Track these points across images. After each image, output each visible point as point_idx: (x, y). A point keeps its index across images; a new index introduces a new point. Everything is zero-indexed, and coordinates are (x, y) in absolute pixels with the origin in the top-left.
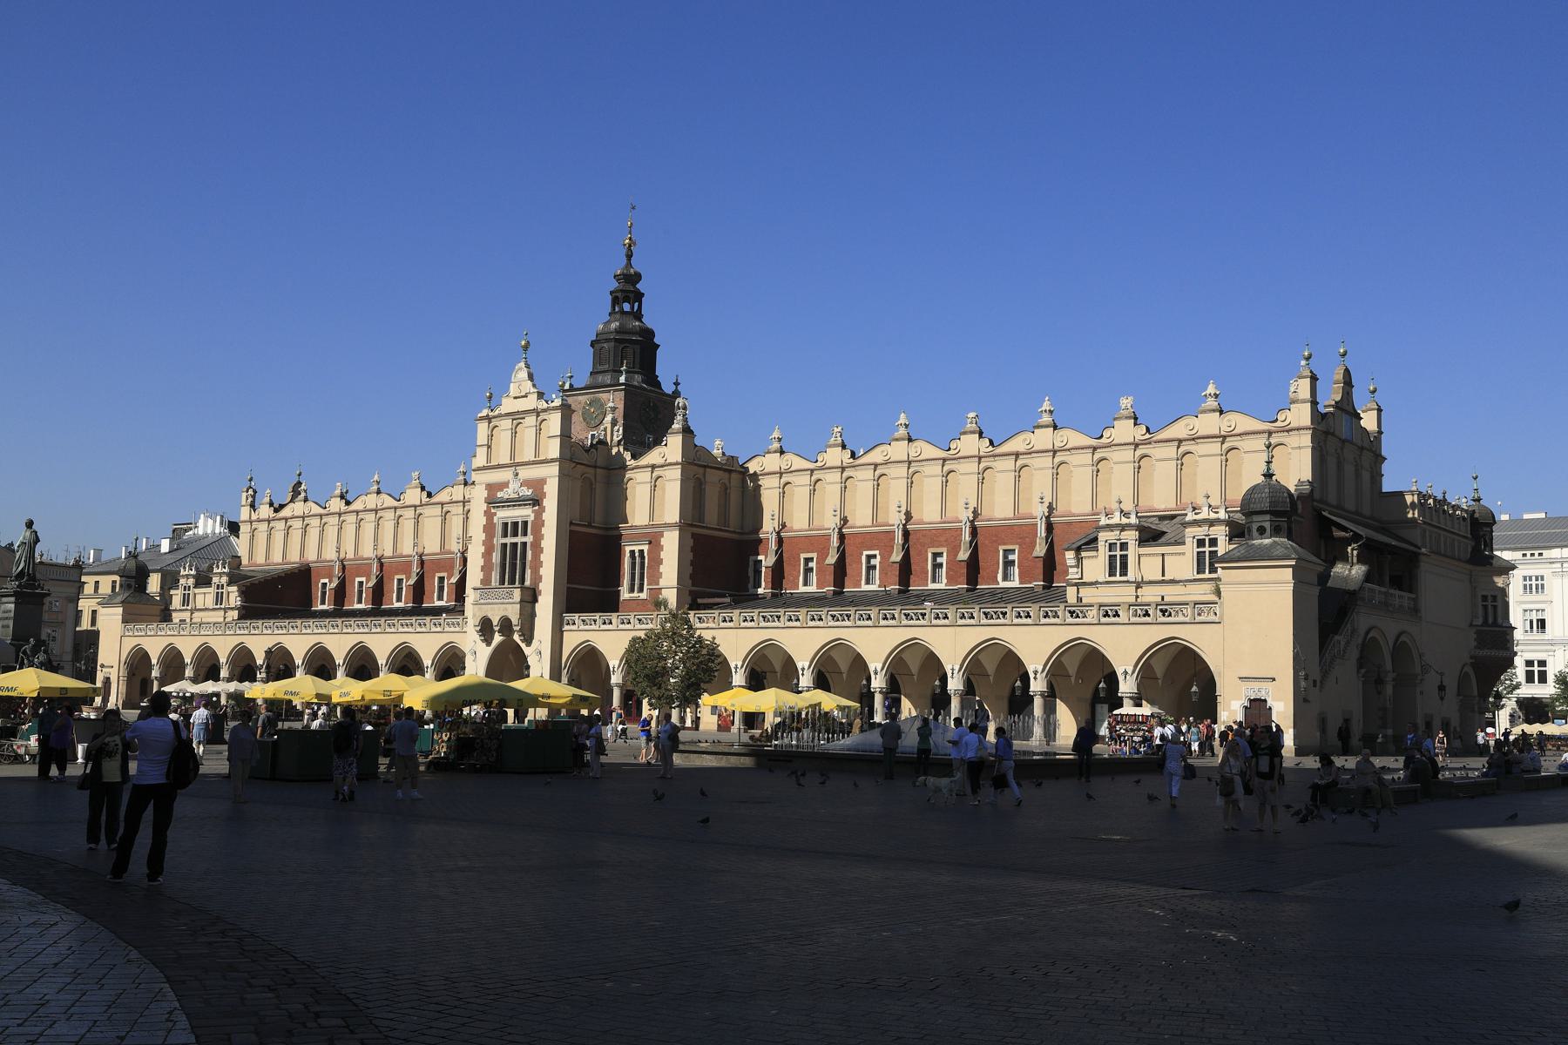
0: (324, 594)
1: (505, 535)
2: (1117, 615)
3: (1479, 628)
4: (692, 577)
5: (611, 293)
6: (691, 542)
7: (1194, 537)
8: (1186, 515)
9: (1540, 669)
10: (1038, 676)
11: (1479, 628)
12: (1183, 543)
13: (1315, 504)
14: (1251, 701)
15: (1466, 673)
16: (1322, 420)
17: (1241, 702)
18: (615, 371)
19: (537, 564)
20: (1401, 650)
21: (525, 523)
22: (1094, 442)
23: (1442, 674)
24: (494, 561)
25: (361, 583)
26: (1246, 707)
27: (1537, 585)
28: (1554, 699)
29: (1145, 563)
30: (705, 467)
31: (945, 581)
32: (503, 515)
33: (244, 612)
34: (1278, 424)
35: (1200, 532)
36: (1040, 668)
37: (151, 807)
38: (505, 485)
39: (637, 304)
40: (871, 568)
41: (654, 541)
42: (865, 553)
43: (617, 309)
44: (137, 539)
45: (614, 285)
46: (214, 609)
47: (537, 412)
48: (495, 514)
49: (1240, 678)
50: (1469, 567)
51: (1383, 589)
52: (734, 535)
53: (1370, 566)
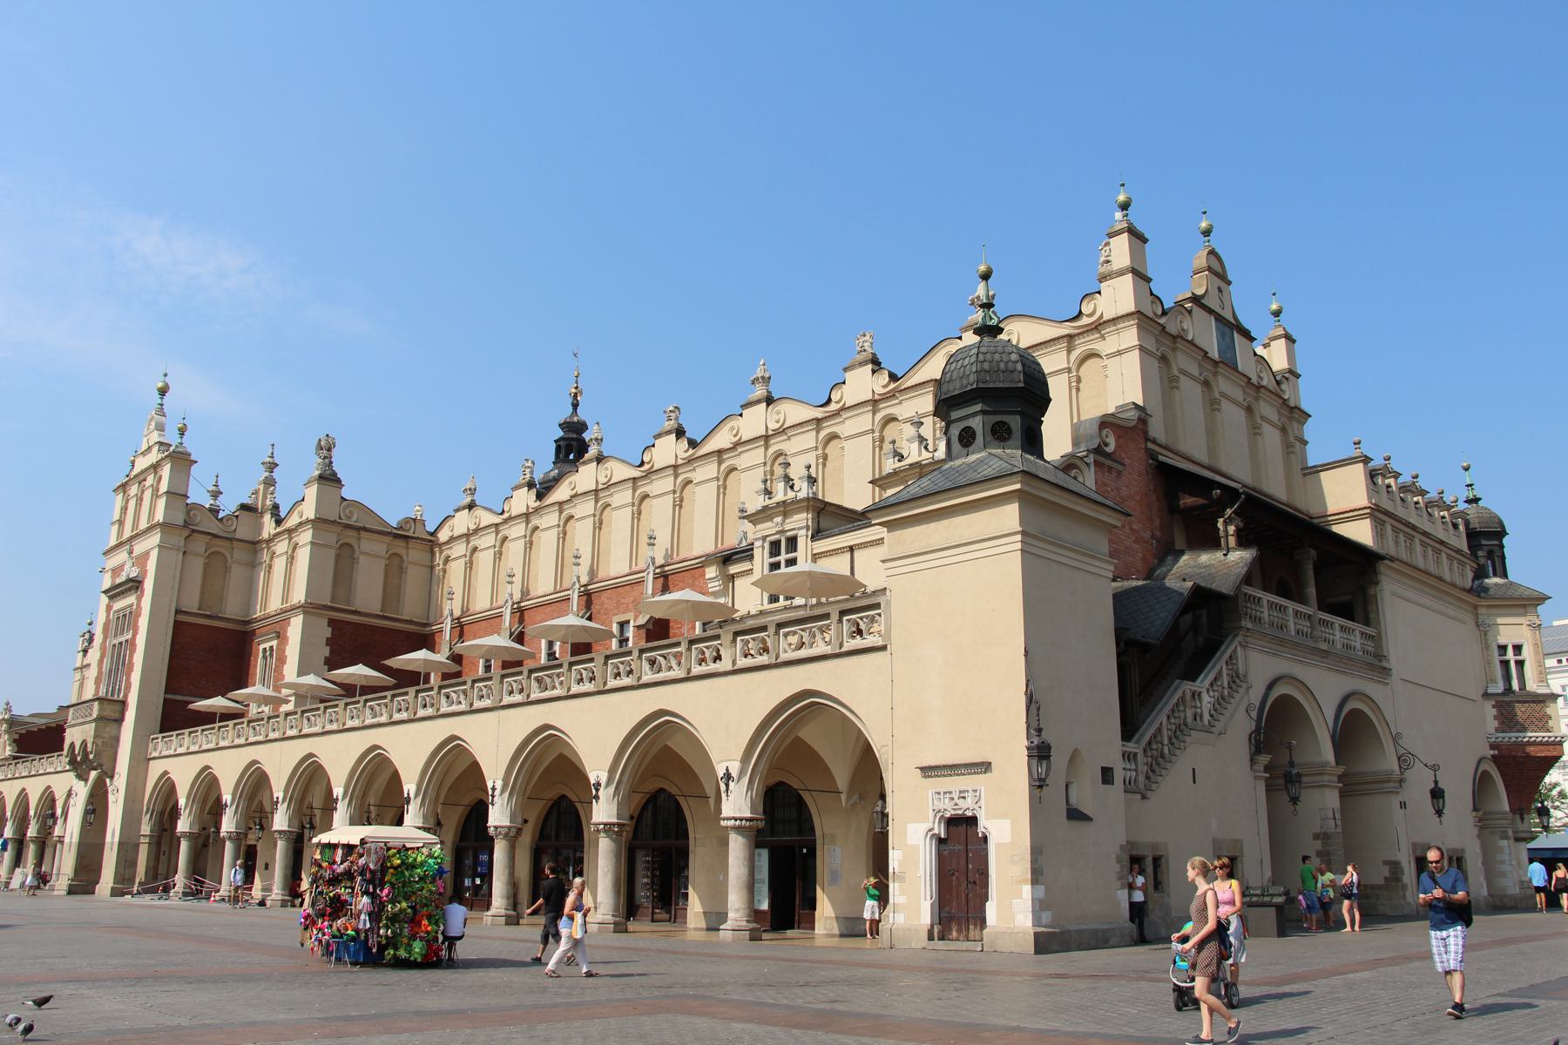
2: (718, 658)
3: (1500, 699)
6: (328, 632)
11: (1500, 699)
13: (1150, 445)
15: (1485, 774)
17: (930, 825)
22: (819, 413)
23: (1435, 768)
26: (941, 841)
30: (359, 529)
34: (1085, 321)
38: (121, 567)
45: (560, 433)
49: (923, 769)
53: (1259, 550)
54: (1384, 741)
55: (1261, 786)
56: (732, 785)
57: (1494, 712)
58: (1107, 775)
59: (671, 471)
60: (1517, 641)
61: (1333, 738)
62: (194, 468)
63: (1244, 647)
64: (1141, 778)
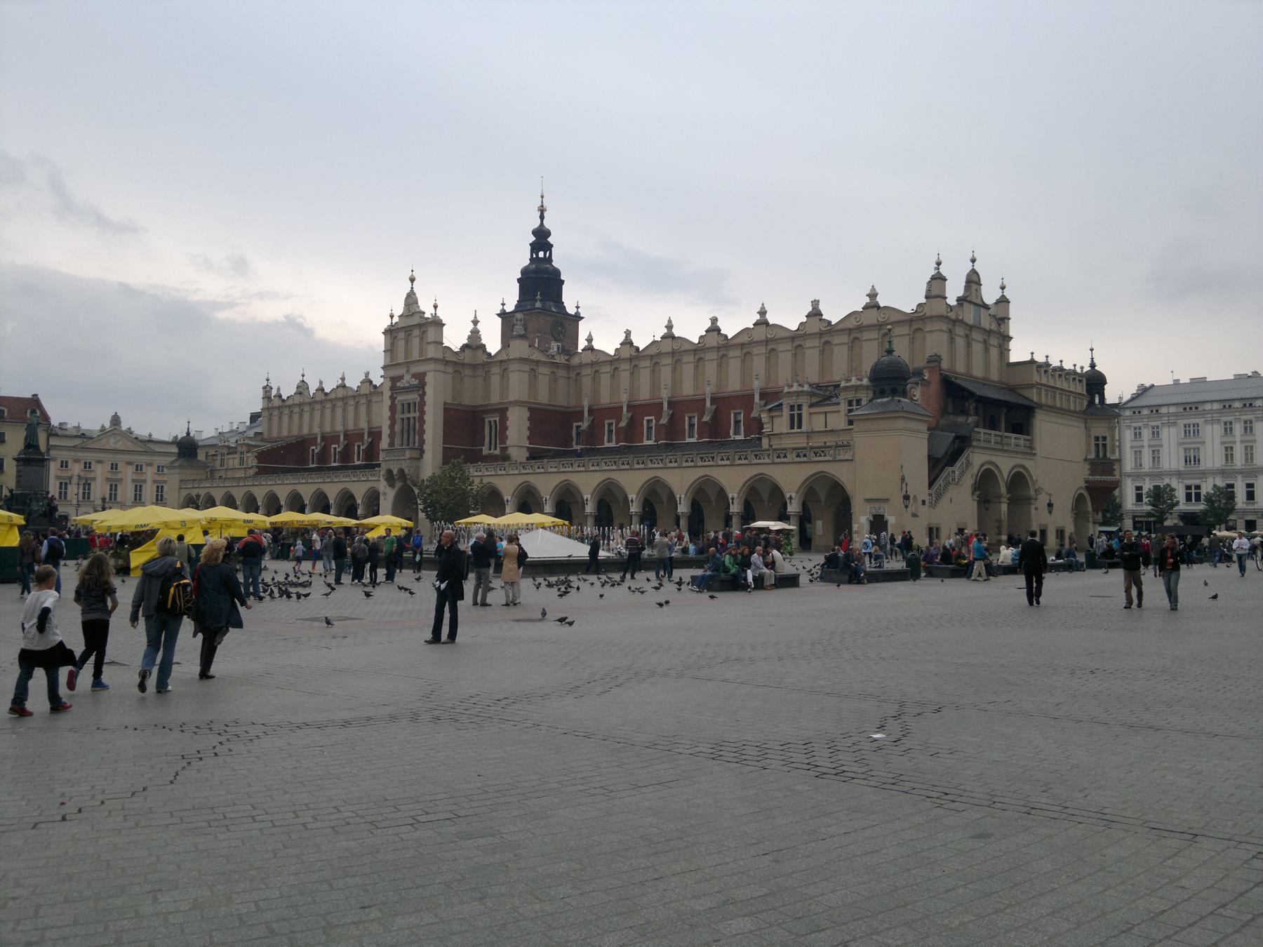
0: (313, 456)
1: (403, 413)
2: (785, 456)
4: (529, 438)
5: (531, 245)
6: (528, 414)
7: (845, 399)
8: (840, 385)
9: (1190, 491)
10: (735, 501)
12: (839, 404)
14: (875, 516)
16: (951, 310)
18: (531, 300)
19: (422, 432)
20: (1019, 480)
21: (415, 403)
24: (396, 430)
25: (335, 448)
26: (871, 523)
27: (1194, 431)
28: (1205, 513)
29: (814, 421)
30: (538, 362)
31: (696, 436)
32: (400, 398)
33: (257, 470)
35: (850, 395)
36: (735, 496)
37: (236, 600)
38: (401, 377)
39: (548, 253)
40: (649, 428)
41: (502, 412)
42: (646, 418)
43: (534, 256)
44: (189, 422)
45: (535, 239)
46: (238, 469)
47: (420, 326)
48: (396, 398)
49: (868, 500)
50: (1085, 417)
51: (997, 433)
52: (563, 409)
54: (1030, 483)
55: (975, 503)
56: (792, 501)
57: (1089, 467)
58: (924, 502)
59: (716, 349)
60: (1104, 435)
61: (1006, 484)
62: (444, 328)
63: (972, 452)
64: (934, 502)
